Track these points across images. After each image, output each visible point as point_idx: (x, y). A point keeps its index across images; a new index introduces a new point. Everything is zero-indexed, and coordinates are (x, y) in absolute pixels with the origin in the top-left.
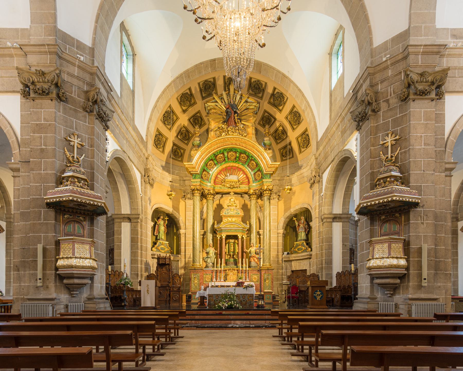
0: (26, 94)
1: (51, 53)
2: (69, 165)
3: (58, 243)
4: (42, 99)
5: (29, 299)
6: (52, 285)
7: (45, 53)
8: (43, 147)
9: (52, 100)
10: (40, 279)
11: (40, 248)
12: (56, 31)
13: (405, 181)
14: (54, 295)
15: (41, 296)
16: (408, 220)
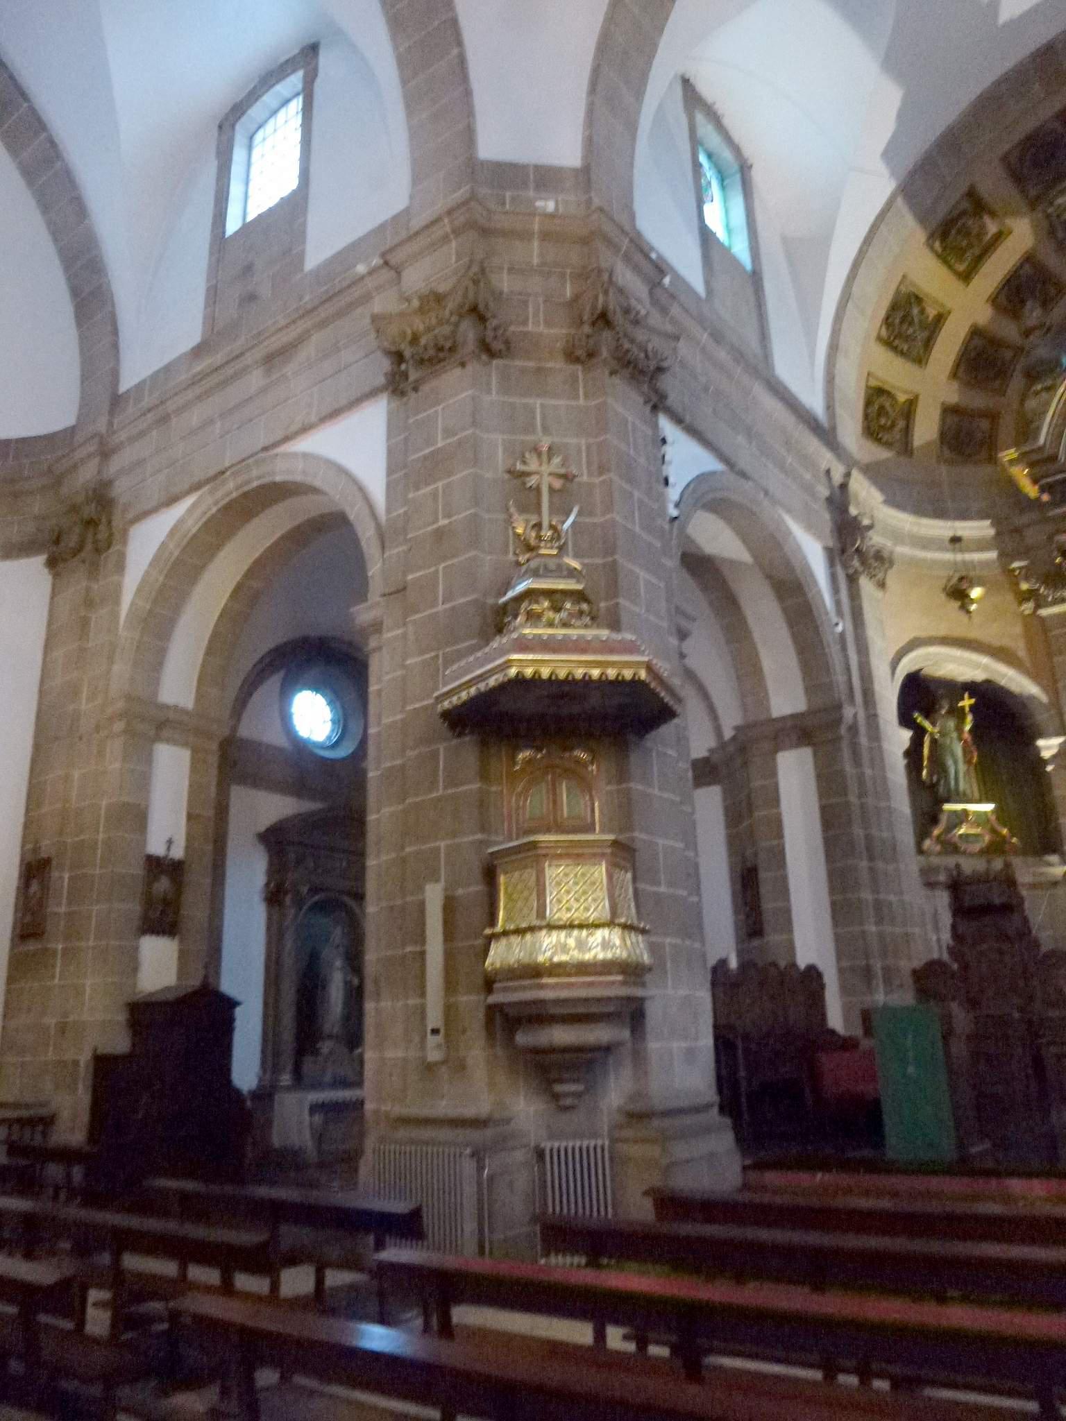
0: (397, 385)
1: (457, 232)
2: (522, 559)
5: (405, 1121)
7: (445, 239)
8: (443, 522)
9: (463, 365)
10: (435, 1031)
11: (434, 895)
12: (473, 168)
14: (482, 1106)
15: (443, 1108)
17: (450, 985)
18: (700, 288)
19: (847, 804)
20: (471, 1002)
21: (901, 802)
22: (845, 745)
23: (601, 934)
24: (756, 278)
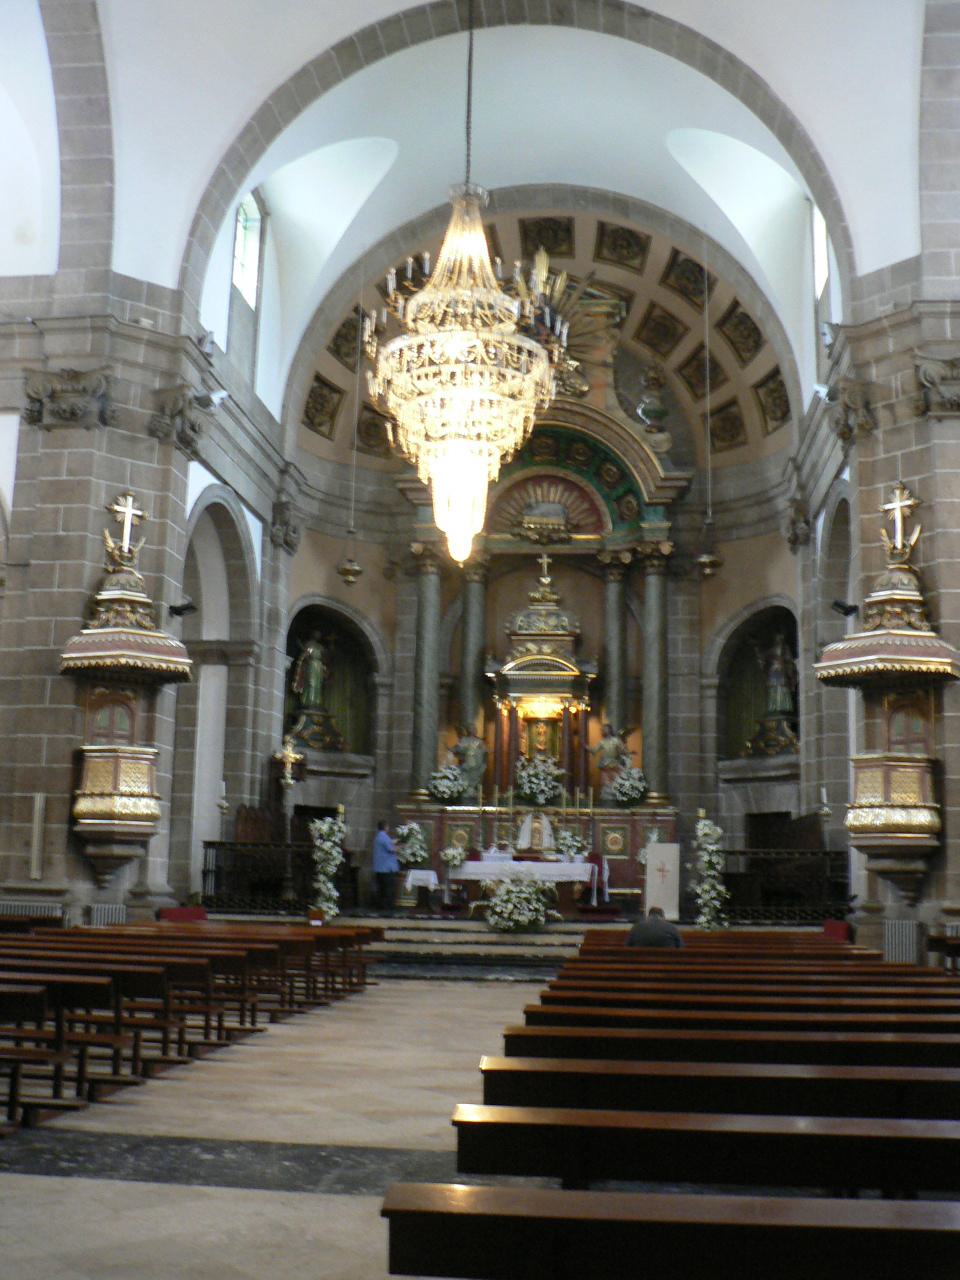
0: (33, 418)
3: (79, 758)
4: (67, 427)
6: (59, 856)
7: (84, 330)
8: (61, 533)
13: (929, 612)
16: (940, 708)
17: (46, 818)
18: (223, 348)
19: (245, 711)
20: (59, 827)
21: (278, 715)
22: (251, 671)
23: (144, 801)
24: (258, 308)
